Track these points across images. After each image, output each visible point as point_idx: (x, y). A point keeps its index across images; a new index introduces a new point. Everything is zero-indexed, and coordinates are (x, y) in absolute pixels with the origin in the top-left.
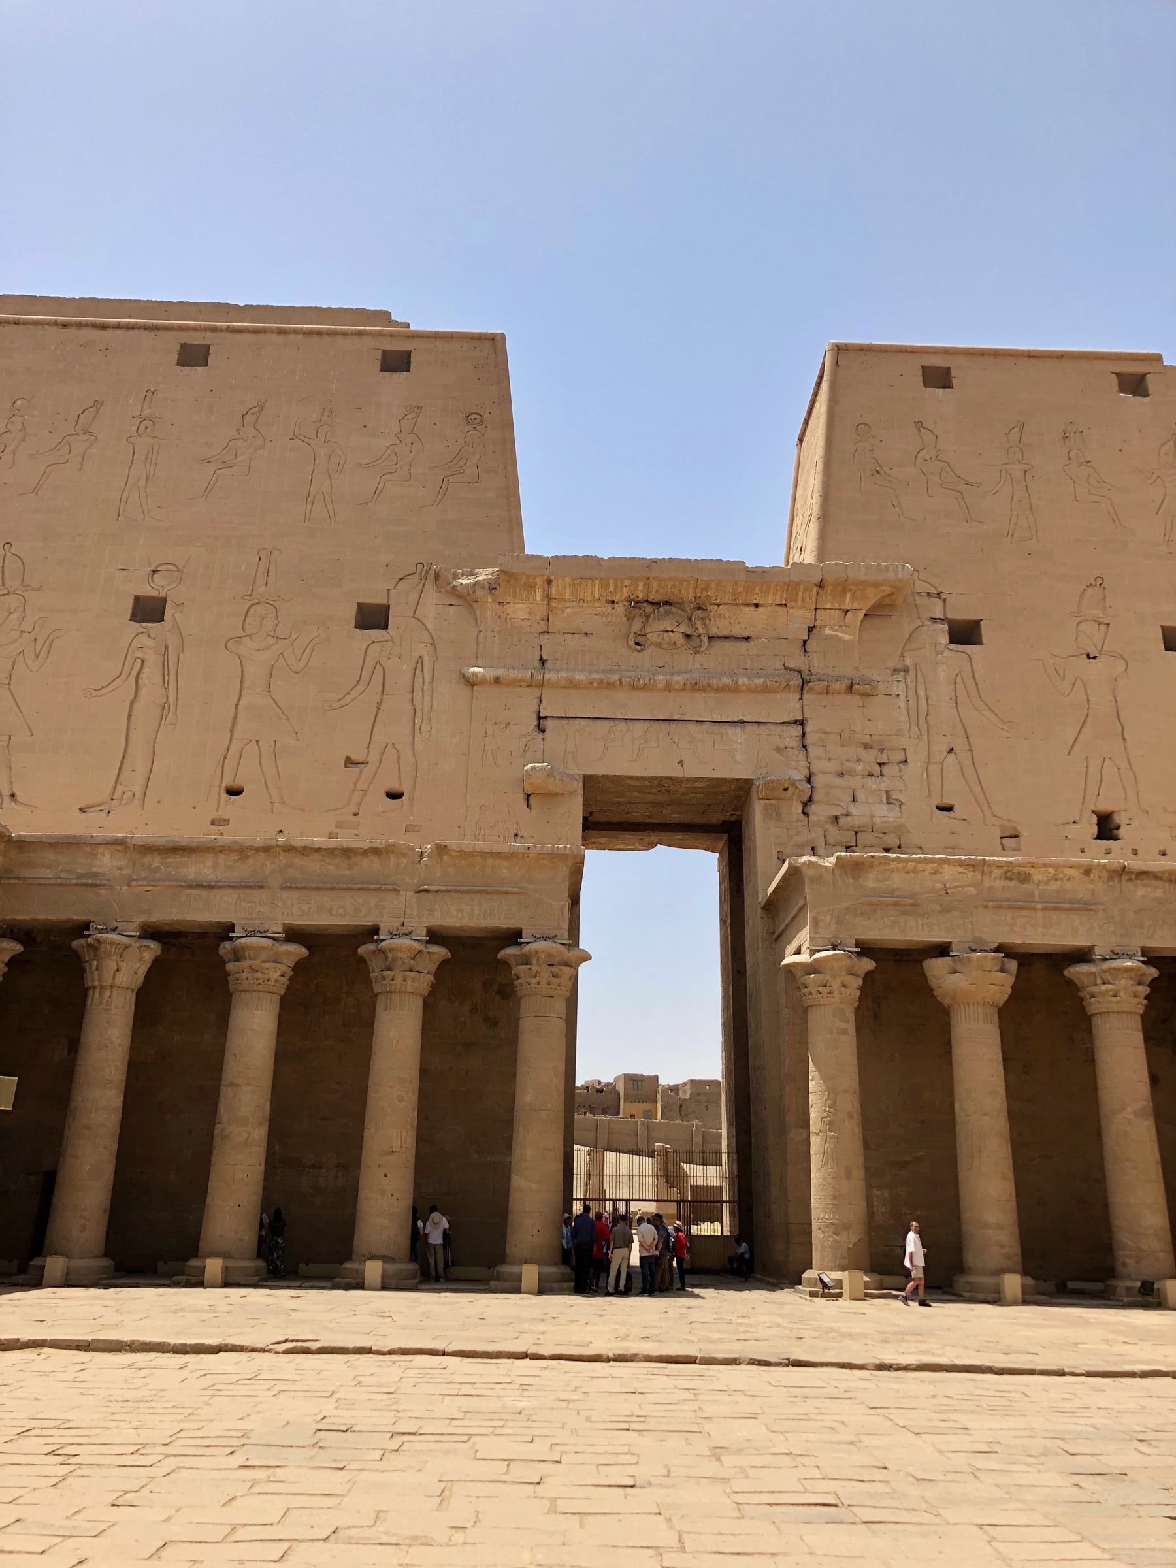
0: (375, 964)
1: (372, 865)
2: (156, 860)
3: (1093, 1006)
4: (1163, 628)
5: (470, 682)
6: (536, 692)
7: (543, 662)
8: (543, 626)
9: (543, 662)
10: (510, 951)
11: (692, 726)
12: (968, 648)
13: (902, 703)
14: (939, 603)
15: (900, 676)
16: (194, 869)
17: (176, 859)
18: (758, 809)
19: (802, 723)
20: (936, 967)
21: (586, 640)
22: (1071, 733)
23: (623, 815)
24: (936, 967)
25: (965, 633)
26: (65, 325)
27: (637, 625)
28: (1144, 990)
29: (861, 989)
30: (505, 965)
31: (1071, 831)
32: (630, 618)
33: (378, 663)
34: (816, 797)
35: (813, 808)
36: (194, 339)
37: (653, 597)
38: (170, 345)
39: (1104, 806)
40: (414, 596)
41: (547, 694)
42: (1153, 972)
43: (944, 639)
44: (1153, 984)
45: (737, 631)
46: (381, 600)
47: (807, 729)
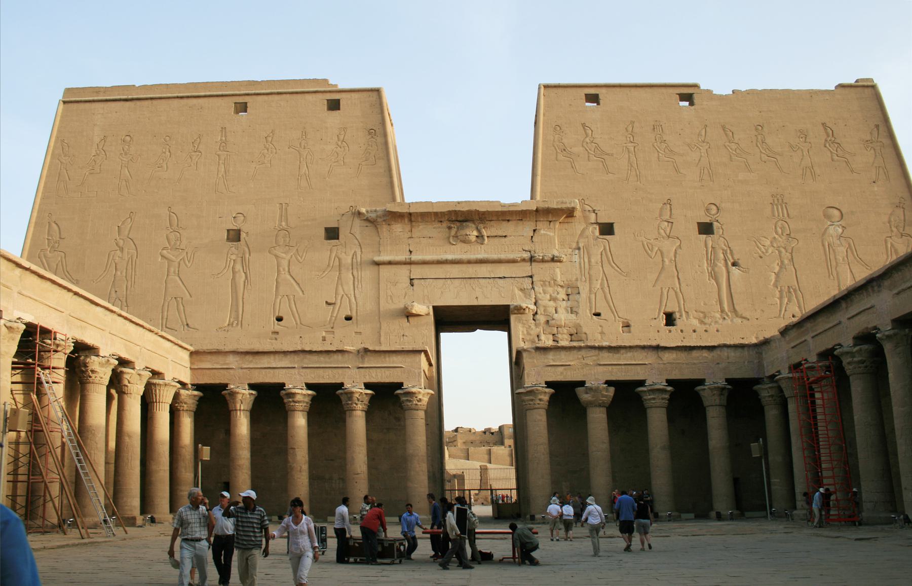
0: (343, 398)
1: (339, 357)
2: (249, 358)
3: (647, 404)
4: (698, 223)
5: (378, 264)
6: (408, 267)
7: (411, 252)
8: (409, 234)
9: (411, 252)
10: (399, 391)
11: (480, 280)
12: (608, 237)
13: (577, 264)
14: (594, 215)
15: (577, 251)
16: (265, 362)
17: (257, 357)
18: (513, 318)
19: (531, 277)
20: (580, 390)
21: (430, 240)
22: (655, 276)
23: (451, 319)
24: (580, 390)
25: (607, 229)
26: (182, 98)
27: (453, 232)
28: (667, 396)
29: (550, 402)
30: (397, 396)
31: (654, 323)
32: (450, 228)
33: (336, 256)
34: (539, 312)
35: (537, 317)
36: (242, 99)
37: (460, 219)
38: (231, 102)
39: (669, 310)
40: (350, 223)
41: (413, 266)
42: (669, 388)
43: (597, 233)
44: (672, 394)
45: (500, 233)
46: (336, 226)
47: (534, 279)
